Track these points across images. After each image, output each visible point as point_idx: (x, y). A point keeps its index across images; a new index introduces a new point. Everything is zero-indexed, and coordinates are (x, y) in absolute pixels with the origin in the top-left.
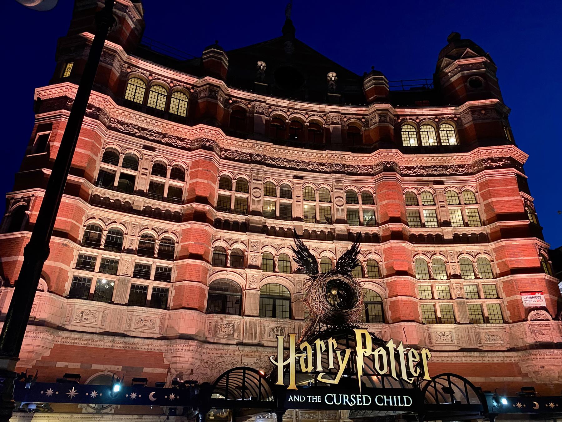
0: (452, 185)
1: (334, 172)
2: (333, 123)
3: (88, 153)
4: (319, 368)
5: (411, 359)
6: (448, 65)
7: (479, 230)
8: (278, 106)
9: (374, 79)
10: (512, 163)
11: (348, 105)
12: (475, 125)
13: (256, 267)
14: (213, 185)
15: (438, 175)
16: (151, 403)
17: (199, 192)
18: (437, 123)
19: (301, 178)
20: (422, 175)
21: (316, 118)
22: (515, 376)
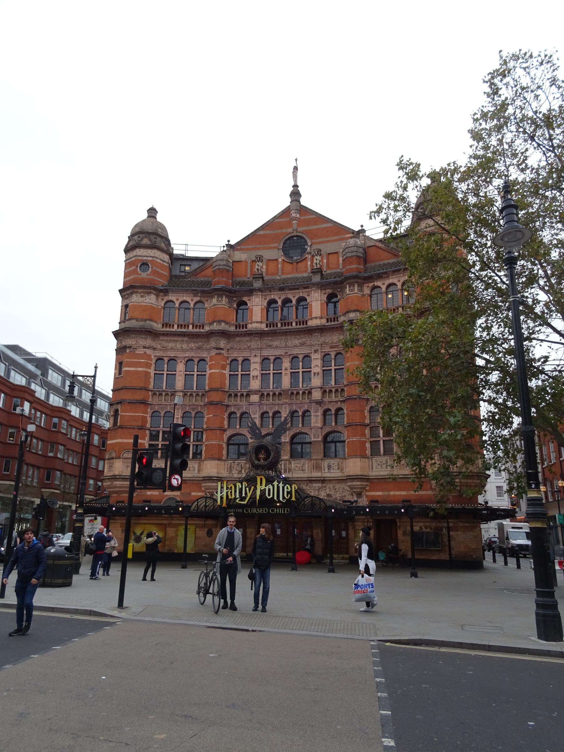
3: (144, 369)
4: (238, 496)
5: (286, 490)
14: (224, 372)
16: (163, 514)
22: (427, 490)
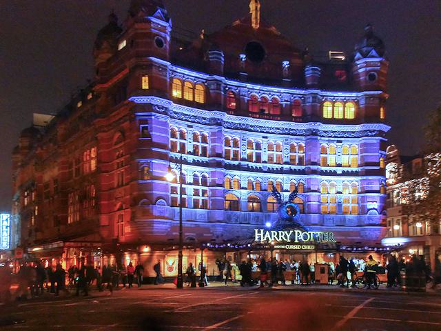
0: (346, 144)
1: (284, 134)
2: (285, 101)
6: (359, 59)
7: (355, 169)
8: (253, 89)
9: (312, 69)
10: (380, 133)
11: (294, 89)
12: (366, 107)
13: (246, 189)
15: (339, 137)
17: (218, 151)
18: (344, 102)
19: (266, 137)
20: (331, 137)
21: (275, 97)
